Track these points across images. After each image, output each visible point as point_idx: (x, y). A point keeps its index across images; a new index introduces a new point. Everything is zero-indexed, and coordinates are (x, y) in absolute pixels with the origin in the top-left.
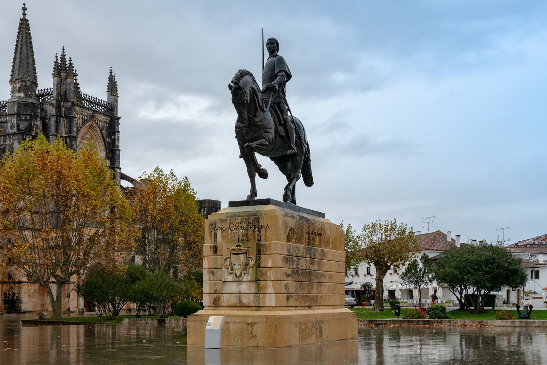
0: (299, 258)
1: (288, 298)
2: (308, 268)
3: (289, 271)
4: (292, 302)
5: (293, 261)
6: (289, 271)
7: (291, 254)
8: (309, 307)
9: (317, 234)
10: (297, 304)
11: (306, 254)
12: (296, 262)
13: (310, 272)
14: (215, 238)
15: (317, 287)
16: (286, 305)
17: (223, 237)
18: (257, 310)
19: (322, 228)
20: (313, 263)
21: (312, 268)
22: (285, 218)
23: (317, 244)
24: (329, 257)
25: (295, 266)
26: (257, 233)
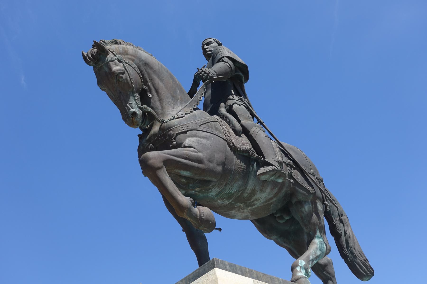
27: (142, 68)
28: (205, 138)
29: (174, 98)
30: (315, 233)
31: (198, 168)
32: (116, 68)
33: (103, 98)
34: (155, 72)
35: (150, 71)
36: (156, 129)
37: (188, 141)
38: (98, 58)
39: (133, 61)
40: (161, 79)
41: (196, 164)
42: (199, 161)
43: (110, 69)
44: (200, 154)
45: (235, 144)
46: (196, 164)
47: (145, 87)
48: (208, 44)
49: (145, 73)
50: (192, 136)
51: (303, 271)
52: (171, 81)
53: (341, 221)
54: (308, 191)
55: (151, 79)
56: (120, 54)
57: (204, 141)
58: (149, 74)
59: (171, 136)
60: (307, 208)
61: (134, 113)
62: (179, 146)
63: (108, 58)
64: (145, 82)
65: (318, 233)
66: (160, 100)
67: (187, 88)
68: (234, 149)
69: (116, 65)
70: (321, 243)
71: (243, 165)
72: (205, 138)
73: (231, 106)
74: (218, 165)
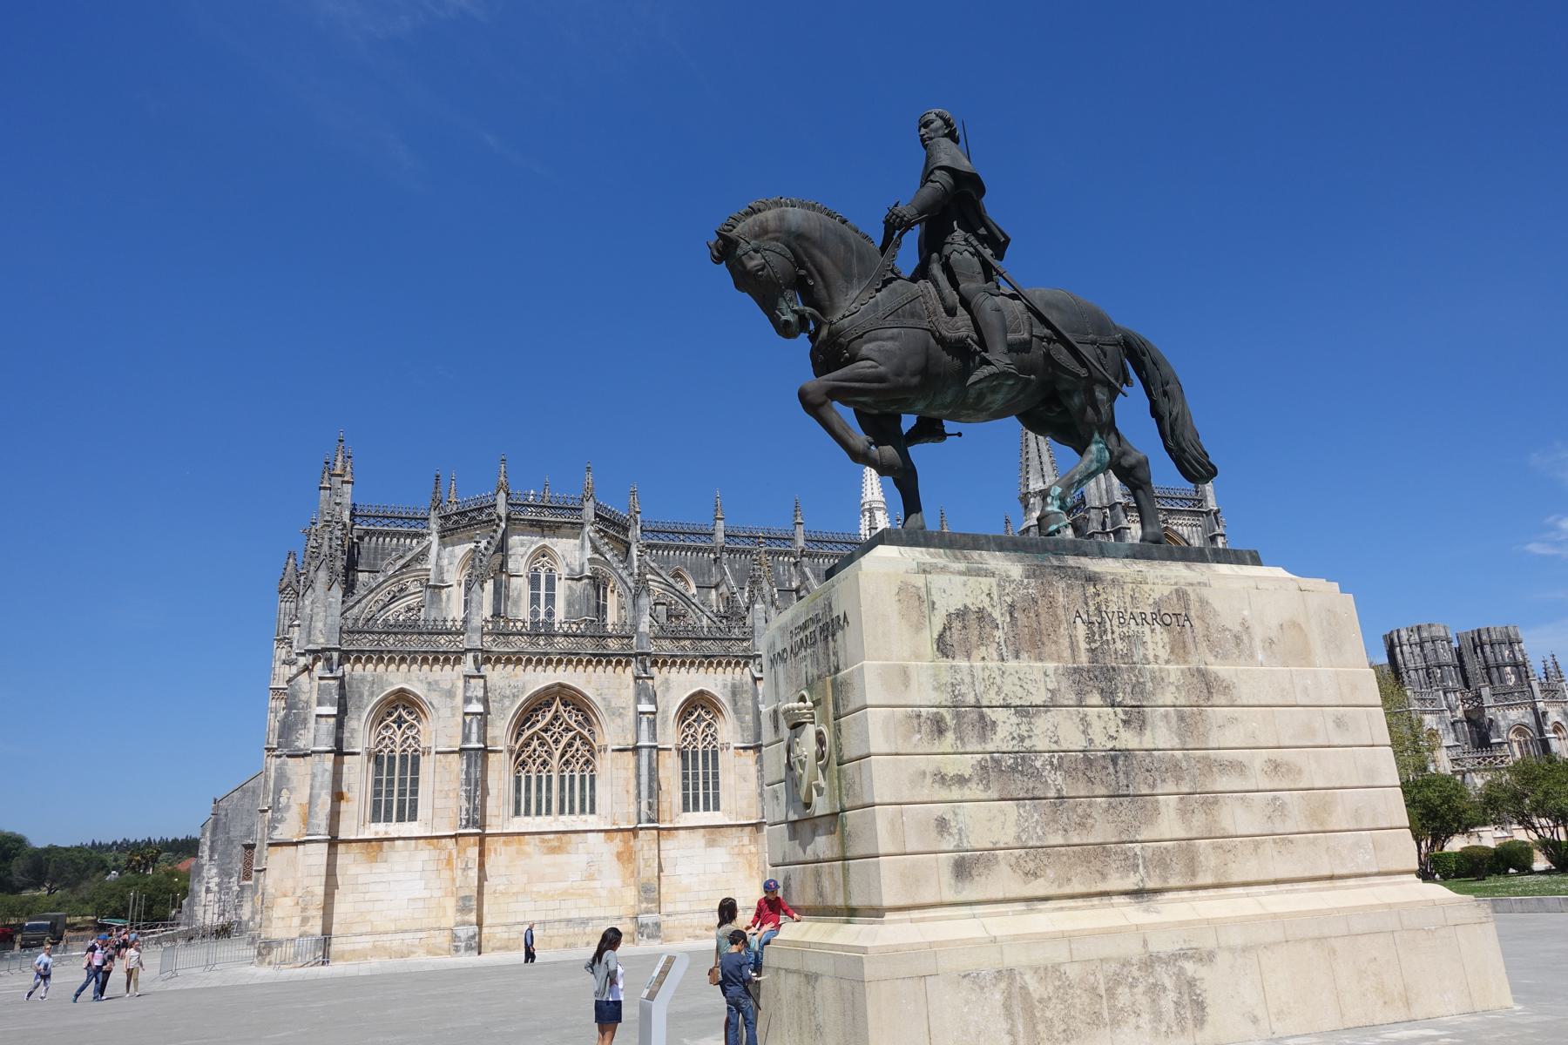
0: (1023, 711)
1: (962, 869)
2: (1101, 742)
3: (965, 765)
4: (1003, 881)
5: (985, 727)
6: (965, 765)
7: (971, 700)
8: (1137, 893)
9: (1159, 617)
10: (1039, 887)
11: (1081, 694)
12: (1002, 732)
13: (1117, 756)
14: (777, 685)
15: (1184, 813)
16: (949, 896)
17: (788, 677)
18: (848, 922)
19: (1181, 595)
20: (1135, 718)
21: (1128, 739)
22: (920, 581)
23: (1163, 654)
24: (1244, 694)
25: (1000, 740)
26: (831, 644)
27: (794, 244)
28: (892, 338)
29: (848, 278)
30: (1092, 436)
31: (879, 390)
32: (754, 263)
33: (747, 302)
34: (814, 243)
35: (806, 245)
36: (824, 332)
37: (866, 349)
38: (726, 250)
39: (777, 239)
40: (826, 253)
41: (875, 385)
42: (881, 378)
43: (744, 266)
44: (882, 369)
45: (944, 333)
46: (875, 385)
47: (803, 272)
48: (926, 125)
49: (800, 251)
50: (870, 341)
51: (1057, 503)
52: (842, 248)
53: (1165, 394)
54: (1077, 376)
55: (811, 258)
56: (756, 237)
57: (889, 345)
58: (805, 250)
59: (841, 345)
60: (1077, 400)
61: (787, 322)
62: (853, 359)
63: (739, 252)
64: (802, 265)
65: (1097, 436)
66: (827, 287)
67: (879, 242)
68: (941, 340)
69: (751, 258)
70: (1099, 451)
71: (957, 362)
72: (892, 338)
73: (948, 258)
74: (913, 375)
